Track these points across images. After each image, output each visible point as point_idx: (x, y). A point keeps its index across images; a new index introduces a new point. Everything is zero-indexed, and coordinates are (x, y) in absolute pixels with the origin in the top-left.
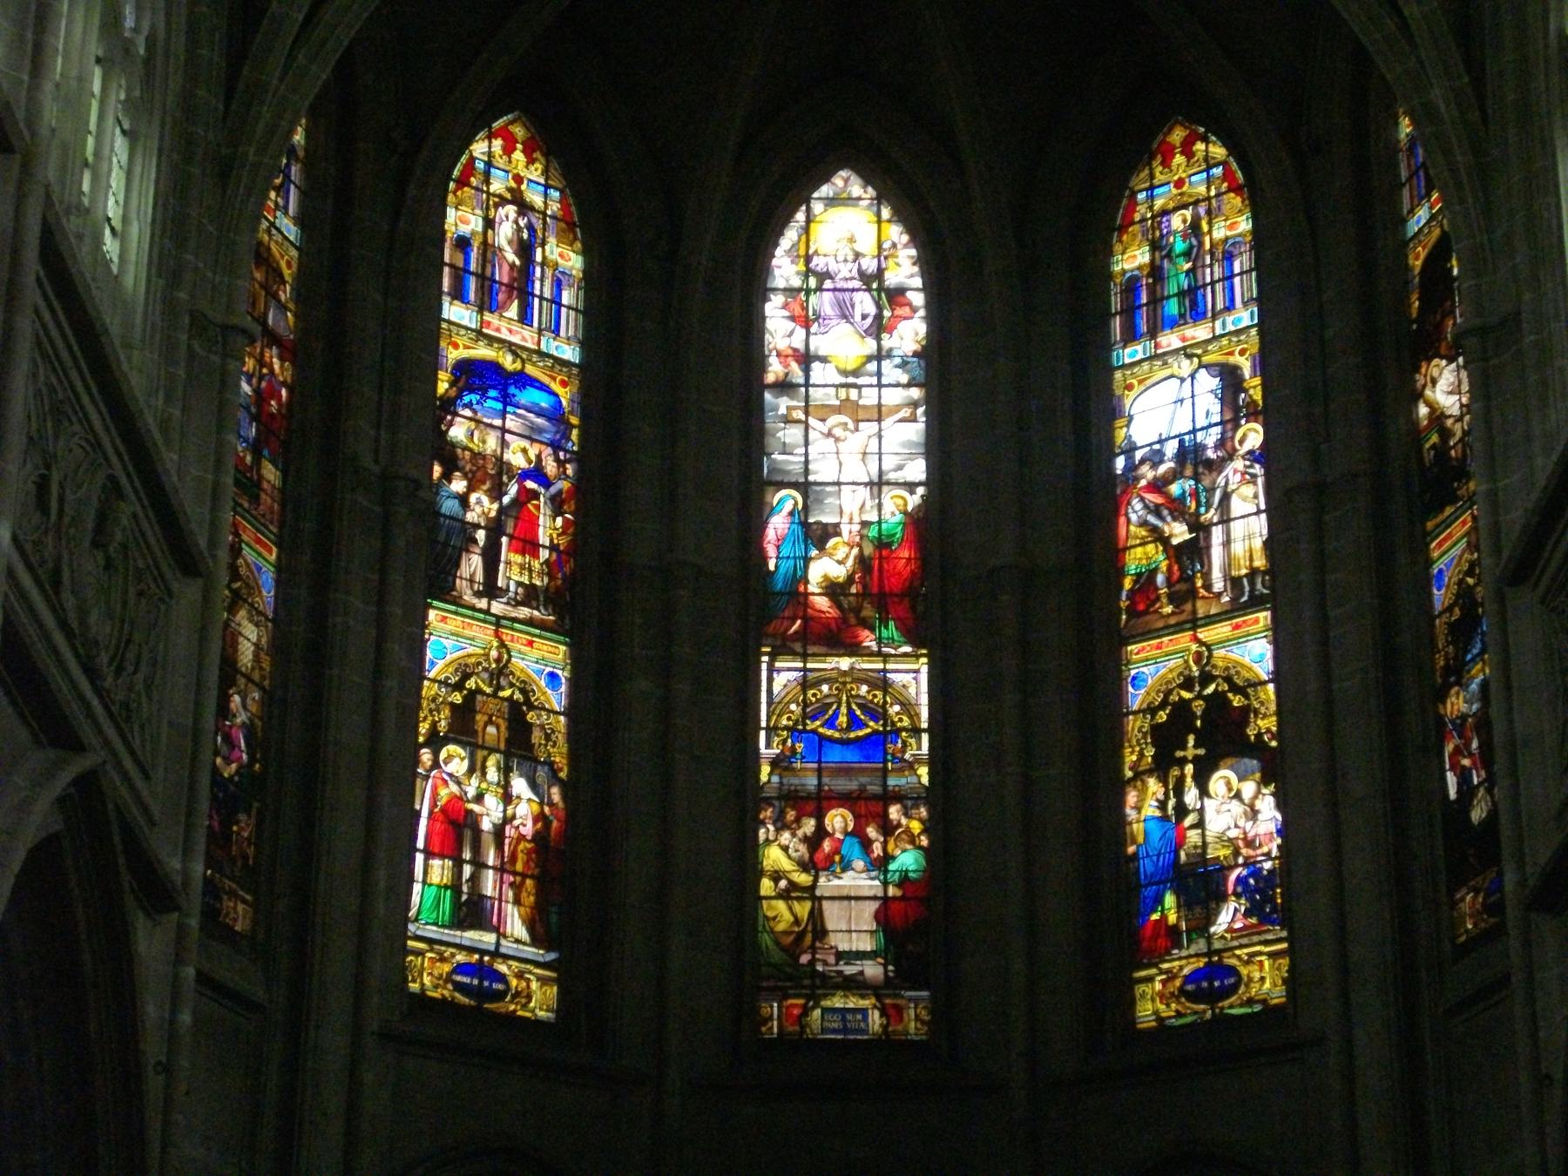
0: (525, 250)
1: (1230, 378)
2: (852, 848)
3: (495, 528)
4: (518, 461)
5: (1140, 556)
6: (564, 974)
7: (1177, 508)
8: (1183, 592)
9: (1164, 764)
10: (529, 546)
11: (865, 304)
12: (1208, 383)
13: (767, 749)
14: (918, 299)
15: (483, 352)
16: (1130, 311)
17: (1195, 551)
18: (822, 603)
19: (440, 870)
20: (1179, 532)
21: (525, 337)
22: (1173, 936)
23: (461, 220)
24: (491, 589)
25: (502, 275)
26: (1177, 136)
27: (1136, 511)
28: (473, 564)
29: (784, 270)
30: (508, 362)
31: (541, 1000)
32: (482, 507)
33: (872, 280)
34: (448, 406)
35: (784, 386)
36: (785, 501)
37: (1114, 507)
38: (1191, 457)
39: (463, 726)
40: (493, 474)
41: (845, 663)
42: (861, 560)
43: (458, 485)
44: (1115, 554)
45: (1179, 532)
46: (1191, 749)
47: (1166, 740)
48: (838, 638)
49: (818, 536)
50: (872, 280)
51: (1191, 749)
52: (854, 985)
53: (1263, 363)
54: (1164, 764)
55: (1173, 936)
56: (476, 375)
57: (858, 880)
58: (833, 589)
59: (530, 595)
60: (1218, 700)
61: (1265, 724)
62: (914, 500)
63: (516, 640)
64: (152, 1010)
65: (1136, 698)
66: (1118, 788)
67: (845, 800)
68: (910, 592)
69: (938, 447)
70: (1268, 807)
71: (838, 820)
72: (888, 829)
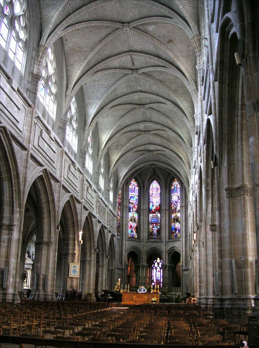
0: (134, 188)
1: (178, 196)
2: (155, 226)
3: (133, 207)
4: (134, 202)
5: (173, 208)
6: (138, 235)
7: (175, 205)
8: (175, 211)
9: (174, 222)
10: (135, 208)
11: (156, 190)
12: (177, 197)
13: (150, 220)
14: (160, 190)
15: (132, 196)
16: (172, 191)
17: (176, 208)
18: (153, 210)
19: (130, 229)
20: (175, 207)
21: (134, 194)
22: (174, 233)
23: (130, 187)
24: (133, 211)
25: (133, 190)
26: (176, 179)
27: (173, 205)
28: (132, 210)
29: (151, 187)
30: (134, 196)
31: (136, 237)
32: (132, 206)
33: (157, 188)
34: (130, 200)
35: (151, 196)
36: (151, 204)
37: (172, 204)
38: (176, 202)
39: (131, 220)
40: (133, 204)
41: (155, 214)
42: (156, 208)
43: (131, 205)
44: (172, 208)
45: (175, 207)
46: (175, 221)
47: (174, 220)
48: (154, 213)
49: (153, 206)
50: (157, 188)
51: (175, 221)
52: (155, 235)
53: (180, 196)
54: (174, 222)
55: (174, 233)
56: (131, 197)
57: (155, 228)
58: (154, 209)
59: (135, 211)
60: (177, 218)
61: (179, 220)
62: (159, 203)
63: (134, 214)
64: (115, 242)
65: (172, 217)
66: (171, 223)
67: (155, 223)
68: (159, 210)
69: (161, 200)
70: (179, 225)
71: (154, 225)
72: (157, 225)
